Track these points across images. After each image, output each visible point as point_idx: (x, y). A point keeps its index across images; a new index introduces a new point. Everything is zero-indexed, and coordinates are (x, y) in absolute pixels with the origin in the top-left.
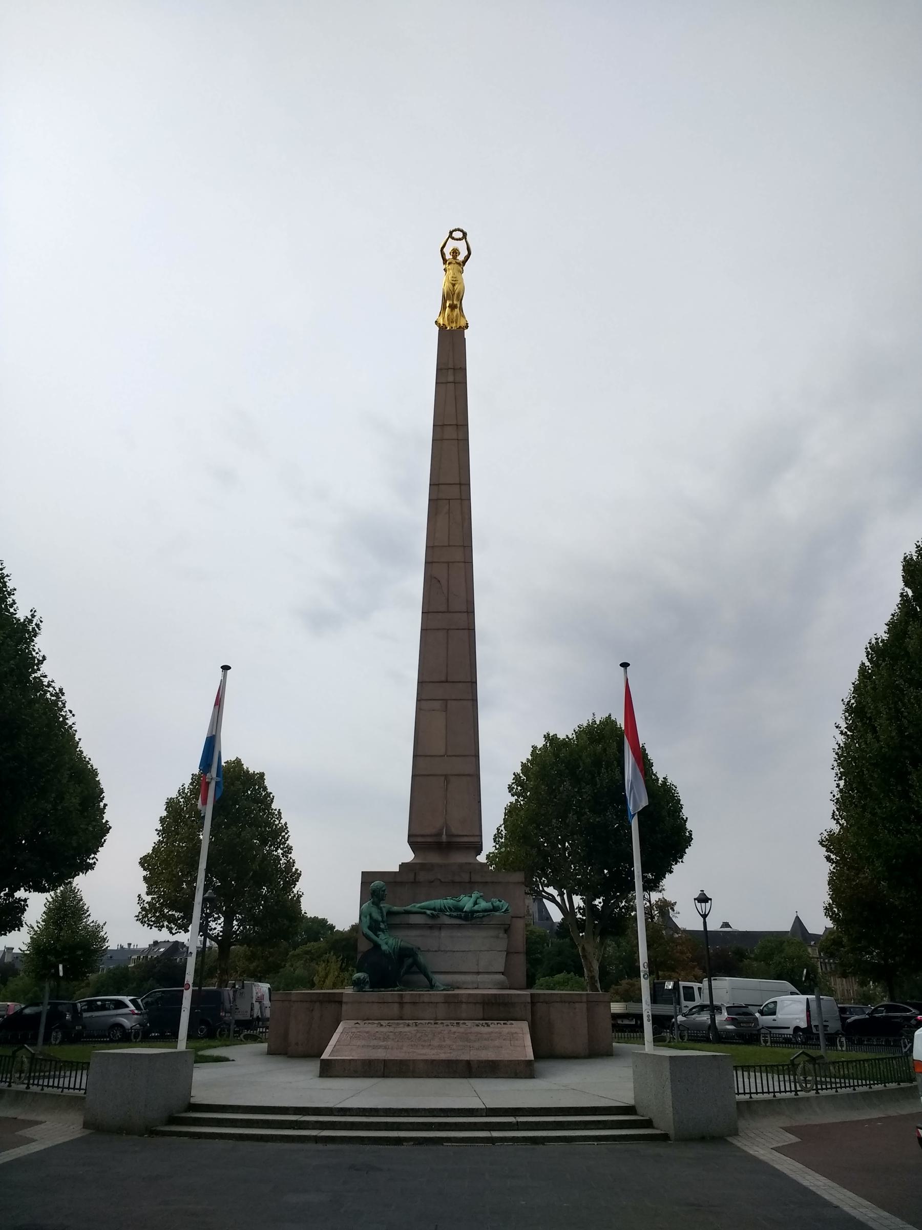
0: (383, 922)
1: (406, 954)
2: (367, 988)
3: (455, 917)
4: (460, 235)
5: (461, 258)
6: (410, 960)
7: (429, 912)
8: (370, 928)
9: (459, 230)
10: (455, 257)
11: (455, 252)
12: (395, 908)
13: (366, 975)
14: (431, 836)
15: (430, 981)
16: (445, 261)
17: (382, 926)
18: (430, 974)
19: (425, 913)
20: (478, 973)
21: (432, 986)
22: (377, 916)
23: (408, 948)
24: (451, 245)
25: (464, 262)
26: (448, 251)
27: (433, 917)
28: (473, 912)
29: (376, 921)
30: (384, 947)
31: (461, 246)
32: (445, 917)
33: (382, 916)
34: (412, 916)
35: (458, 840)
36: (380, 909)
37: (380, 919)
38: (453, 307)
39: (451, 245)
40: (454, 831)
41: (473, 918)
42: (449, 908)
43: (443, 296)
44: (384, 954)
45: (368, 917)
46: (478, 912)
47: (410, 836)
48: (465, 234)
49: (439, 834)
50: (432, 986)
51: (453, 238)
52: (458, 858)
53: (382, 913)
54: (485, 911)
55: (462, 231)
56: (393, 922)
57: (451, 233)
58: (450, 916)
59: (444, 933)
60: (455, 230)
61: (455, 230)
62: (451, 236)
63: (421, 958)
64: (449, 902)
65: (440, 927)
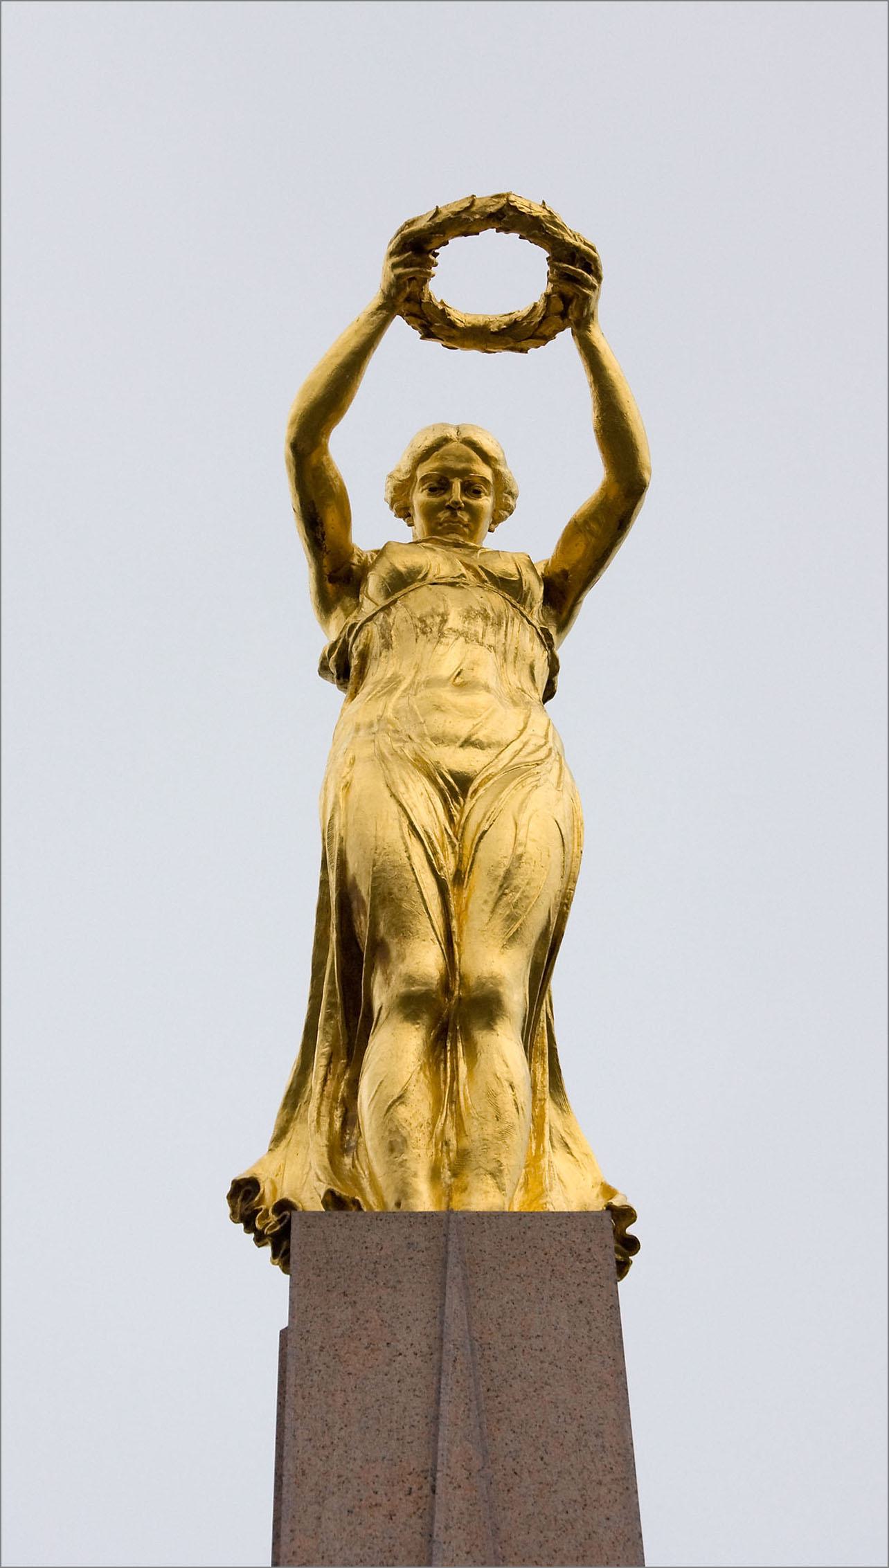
5: (528, 538)
9: (506, 217)
11: (452, 489)
16: (338, 577)
24: (413, 397)
25: (562, 593)
26: (367, 456)
31: (533, 422)
38: (454, 1014)
39: (413, 397)
48: (574, 272)
51: (435, 325)
57: (417, 248)
60: (464, 221)
61: (464, 221)
62: (407, 295)
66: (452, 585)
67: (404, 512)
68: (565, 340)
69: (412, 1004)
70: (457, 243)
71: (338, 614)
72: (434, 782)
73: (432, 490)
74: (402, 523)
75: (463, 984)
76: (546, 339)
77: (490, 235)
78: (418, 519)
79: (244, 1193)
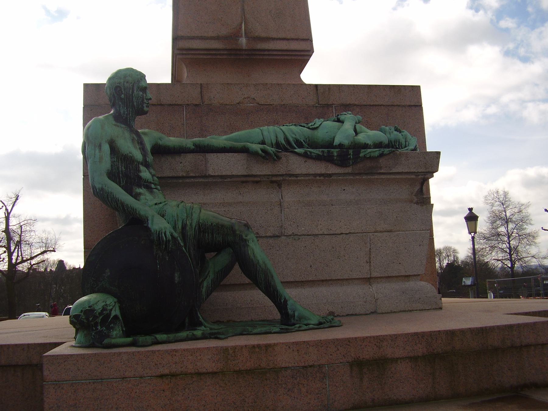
0: (147, 165)
1: (220, 245)
2: (116, 334)
3: (318, 158)
6: (224, 258)
7: (257, 147)
8: (112, 175)
12: (172, 141)
13: (110, 300)
14: (217, 38)
15: (281, 304)
17: (145, 174)
18: (280, 287)
19: (244, 150)
20: (369, 280)
21: (288, 320)
22: (127, 146)
23: (219, 228)
27: (265, 156)
28: (358, 147)
29: (128, 159)
30: (158, 224)
32: (293, 159)
33: (143, 149)
34: (212, 157)
35: (271, 45)
36: (137, 134)
37: (138, 155)
40: (260, 32)
41: (357, 159)
42: (300, 144)
44: (157, 242)
45: (106, 148)
46: (366, 146)
47: (176, 39)
49: (236, 36)
50: (288, 320)
52: (271, 77)
53: (141, 143)
54: (379, 145)
56: (168, 173)
58: (306, 156)
59: (290, 195)
63: (257, 251)
64: (294, 131)
65: (276, 182)
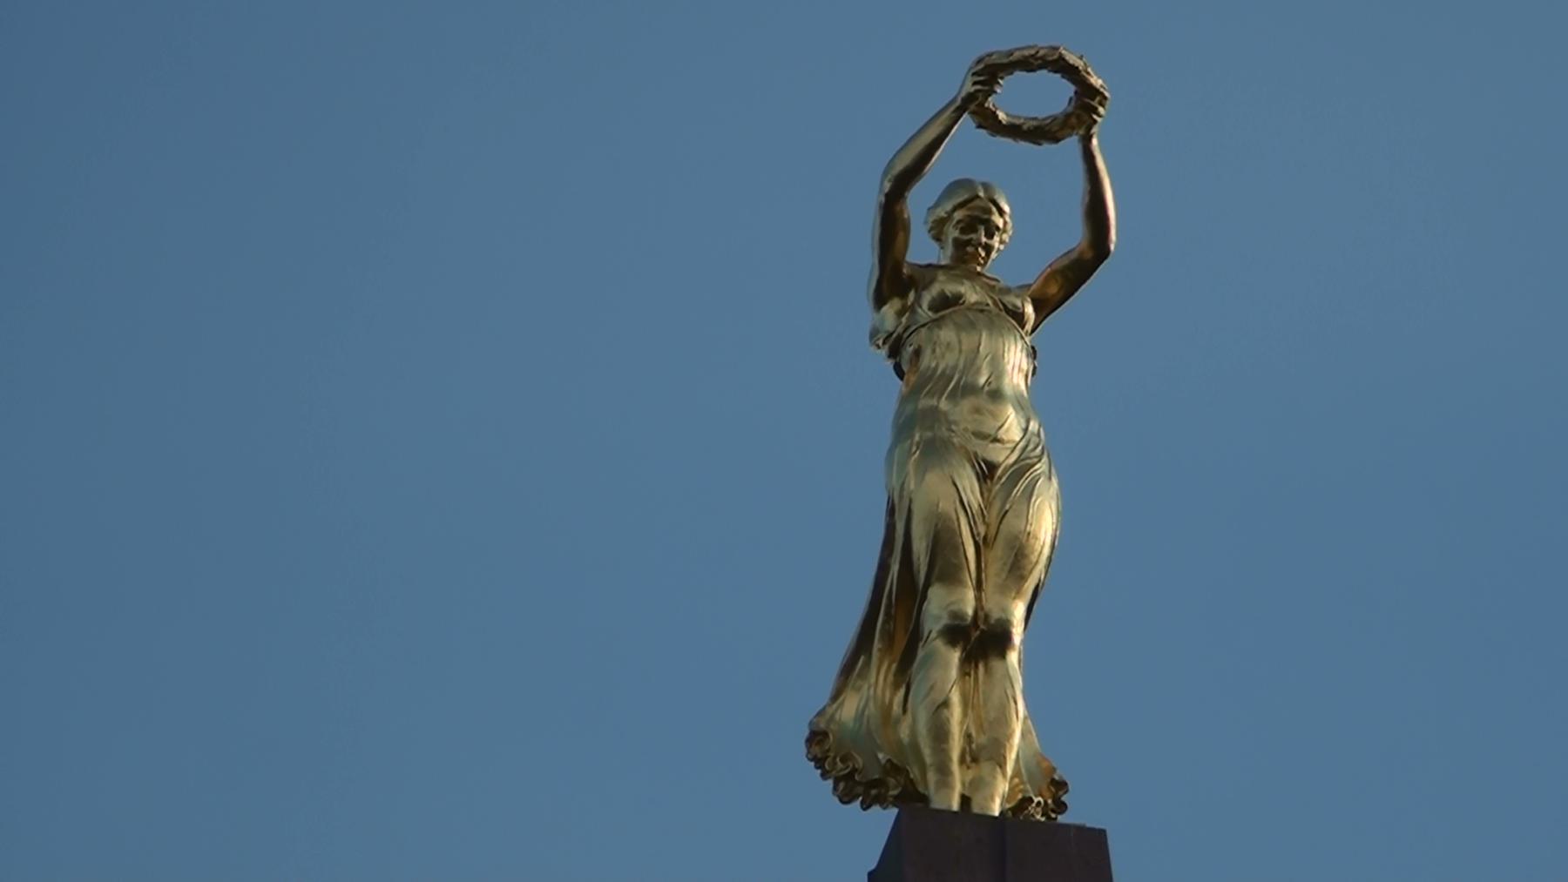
4: (1042, 96)
10: (965, 257)
43: (895, 542)
51: (988, 121)
55: (1071, 73)
57: (990, 73)
61: (1029, 63)
66: (982, 311)
67: (938, 239)
68: (1072, 143)
69: (956, 633)
70: (1019, 75)
71: (889, 310)
72: (970, 461)
73: (963, 231)
74: (935, 245)
75: (987, 617)
76: (1057, 140)
77: (1043, 73)
78: (950, 250)
79: (816, 737)
